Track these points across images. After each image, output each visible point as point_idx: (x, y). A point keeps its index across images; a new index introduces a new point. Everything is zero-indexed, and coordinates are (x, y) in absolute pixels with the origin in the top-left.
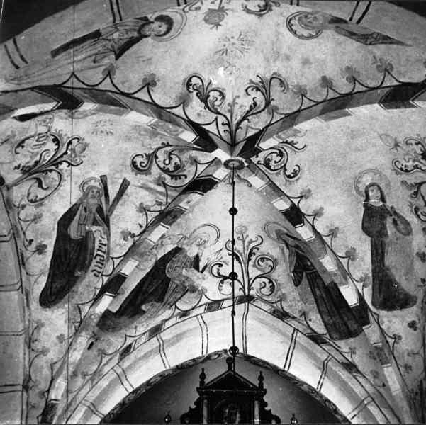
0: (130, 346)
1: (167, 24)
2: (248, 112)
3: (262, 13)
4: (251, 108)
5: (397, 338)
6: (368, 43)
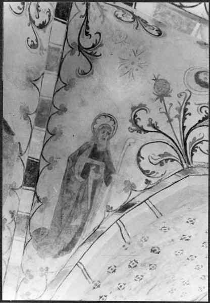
1: (200, 80)
2: (88, 22)
3: (133, 115)
4: (88, 28)
6: (70, 159)
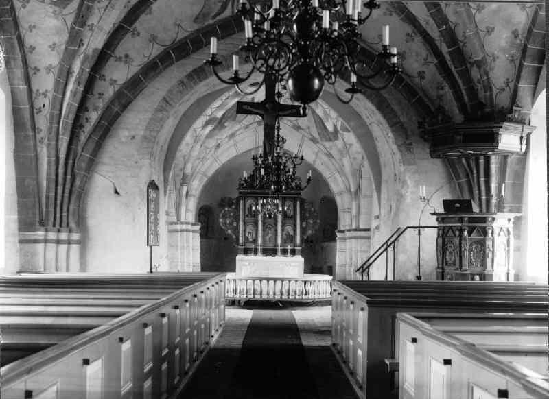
0: (219, 144)
5: (351, 145)
